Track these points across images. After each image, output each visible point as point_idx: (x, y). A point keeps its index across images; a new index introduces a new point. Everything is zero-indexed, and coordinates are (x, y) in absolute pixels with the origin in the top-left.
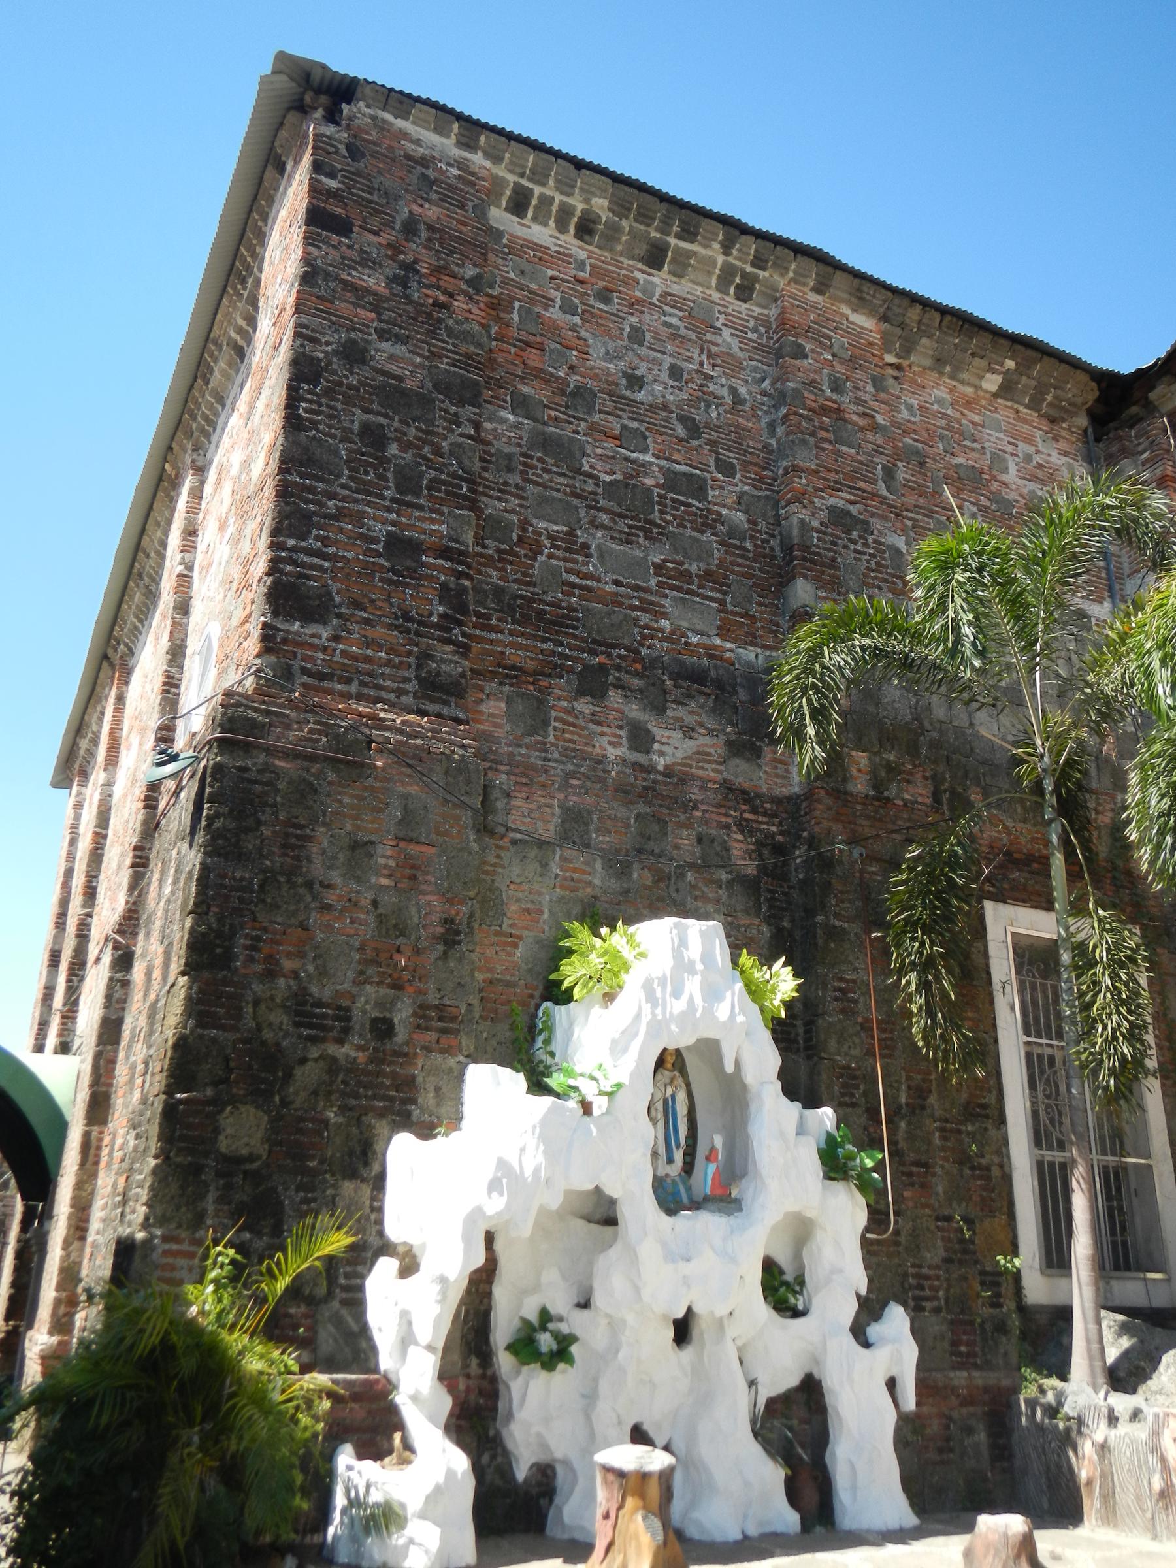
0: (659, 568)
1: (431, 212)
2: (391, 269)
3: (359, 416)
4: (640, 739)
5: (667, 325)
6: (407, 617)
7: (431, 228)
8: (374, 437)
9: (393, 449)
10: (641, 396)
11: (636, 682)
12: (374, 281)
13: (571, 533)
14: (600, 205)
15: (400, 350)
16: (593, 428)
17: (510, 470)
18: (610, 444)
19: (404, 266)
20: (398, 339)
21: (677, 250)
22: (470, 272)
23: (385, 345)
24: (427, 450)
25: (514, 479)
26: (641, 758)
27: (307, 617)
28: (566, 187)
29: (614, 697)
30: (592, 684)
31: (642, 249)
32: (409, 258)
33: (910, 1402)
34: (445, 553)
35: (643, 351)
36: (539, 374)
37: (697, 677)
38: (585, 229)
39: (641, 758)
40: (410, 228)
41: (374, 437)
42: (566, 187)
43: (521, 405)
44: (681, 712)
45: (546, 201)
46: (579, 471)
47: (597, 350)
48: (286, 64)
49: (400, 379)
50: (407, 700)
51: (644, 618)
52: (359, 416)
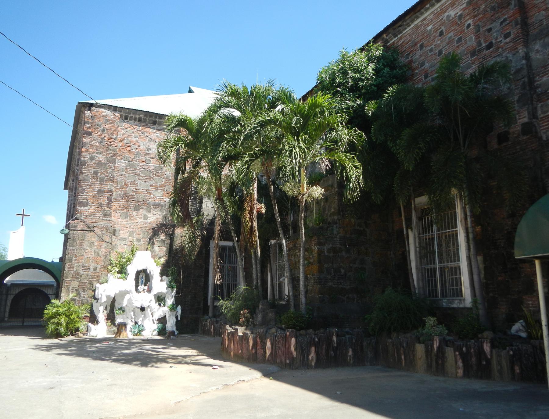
0: (151, 185)
1: (107, 126)
2: (99, 140)
3: (93, 170)
4: (145, 217)
5: (157, 136)
6: (101, 204)
7: (107, 129)
8: (96, 173)
9: (99, 174)
10: (149, 152)
11: (145, 207)
12: (96, 143)
13: (134, 182)
14: (142, 116)
15: (101, 156)
16: (140, 161)
17: (123, 171)
18: (143, 163)
19: (102, 139)
20: (100, 153)
21: (159, 122)
22: (115, 136)
23: (98, 155)
24: (105, 174)
25: (124, 173)
26: (145, 221)
27: (84, 206)
28: (135, 114)
29: (141, 211)
30: (137, 209)
31: (152, 122)
32: (103, 137)
33: (179, 319)
34: (108, 191)
35: (151, 143)
36: (129, 151)
37: (158, 205)
38: (140, 120)
39: (145, 221)
40: (103, 131)
41: (96, 173)
42: (135, 114)
43: (126, 158)
44: (153, 212)
45: (131, 117)
46: (136, 169)
47: (142, 144)
48: (79, 103)
49: (100, 161)
50: (101, 218)
51: (148, 195)
52: (93, 170)
